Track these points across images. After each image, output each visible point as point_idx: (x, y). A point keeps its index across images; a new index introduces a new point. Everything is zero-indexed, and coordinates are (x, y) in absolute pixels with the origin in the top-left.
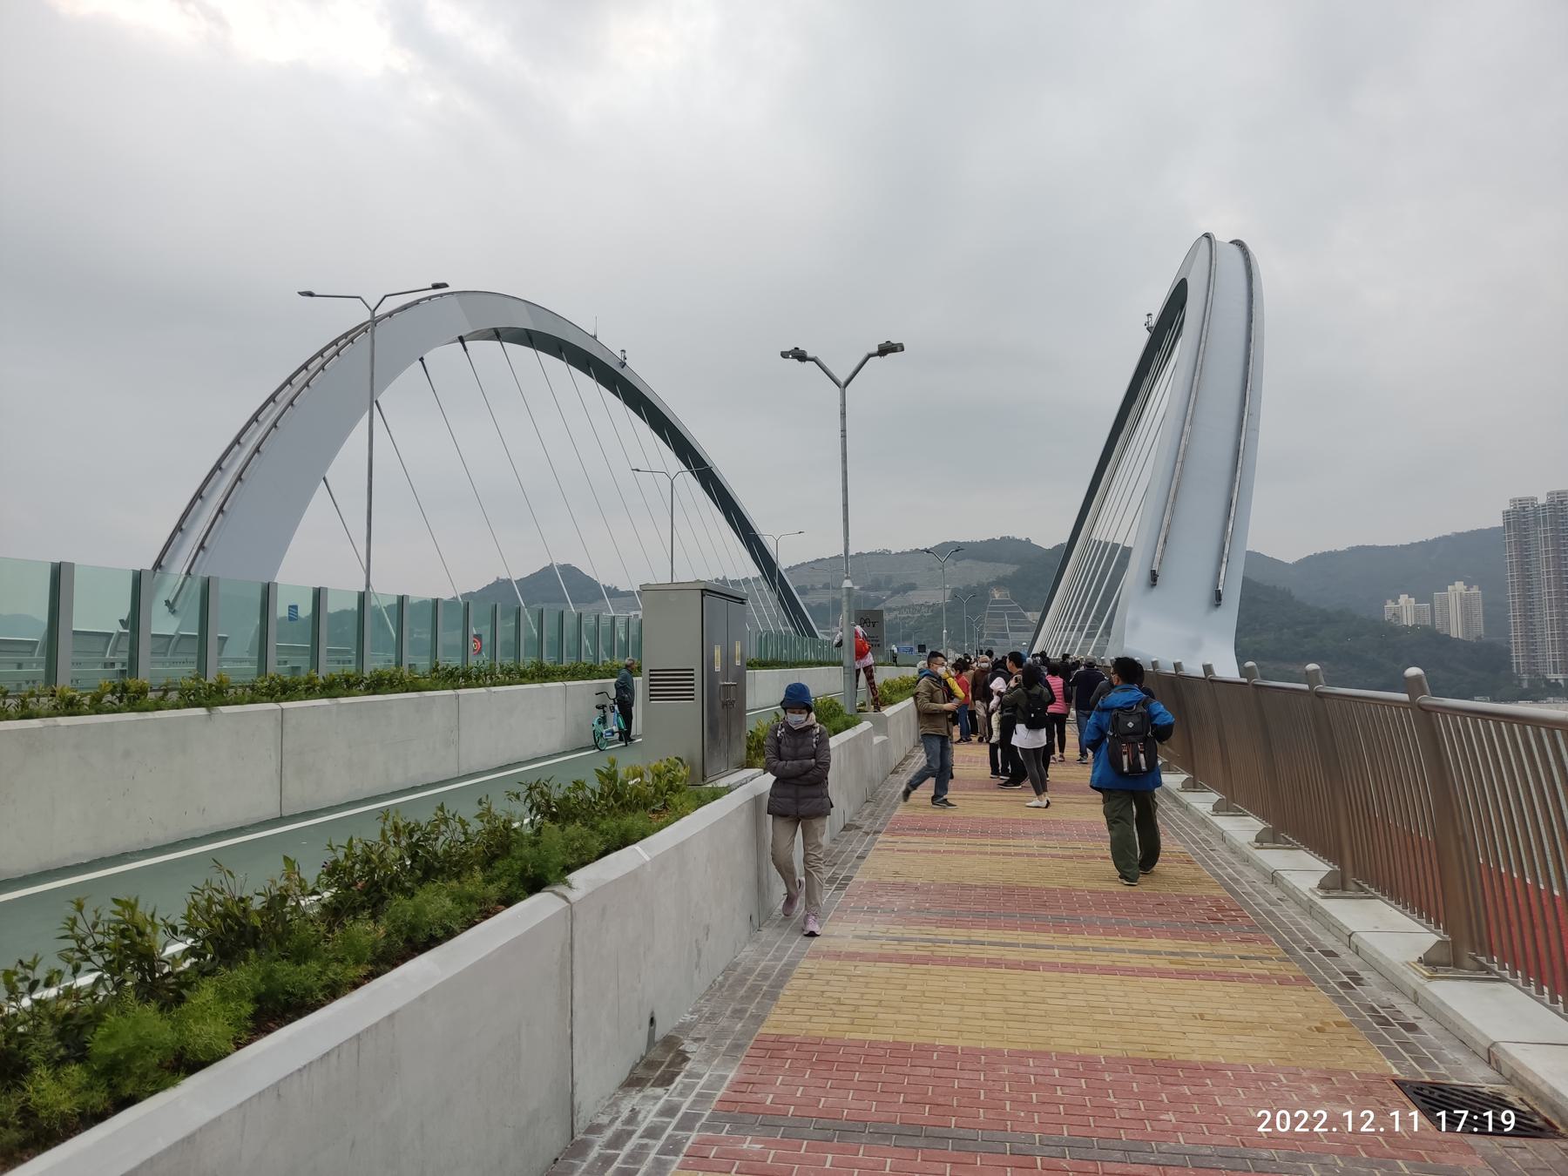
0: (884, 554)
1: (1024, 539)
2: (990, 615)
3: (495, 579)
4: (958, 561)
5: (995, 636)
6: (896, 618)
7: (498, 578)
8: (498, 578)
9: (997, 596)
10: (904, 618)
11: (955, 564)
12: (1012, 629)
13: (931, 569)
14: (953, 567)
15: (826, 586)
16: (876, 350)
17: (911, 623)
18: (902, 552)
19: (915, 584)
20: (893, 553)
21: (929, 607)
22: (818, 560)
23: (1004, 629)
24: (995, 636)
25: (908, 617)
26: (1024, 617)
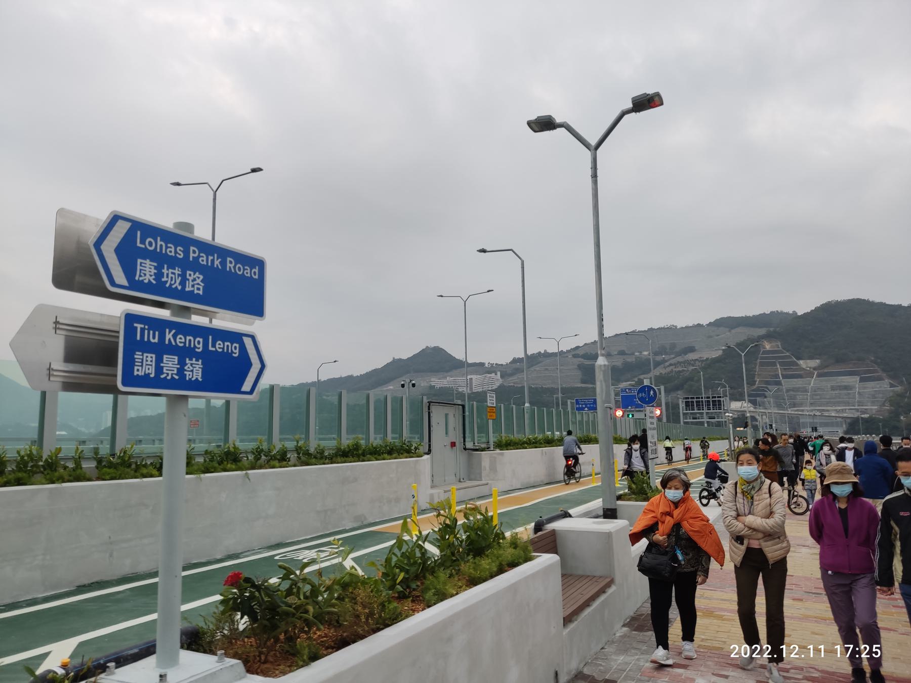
0: (671, 329)
1: (791, 312)
2: (762, 364)
3: (392, 359)
4: (732, 329)
5: (767, 383)
6: (672, 371)
7: (394, 358)
8: (394, 358)
9: (768, 346)
10: (680, 372)
11: (730, 331)
12: (784, 377)
13: (710, 337)
14: (728, 333)
15: (622, 353)
16: (630, 105)
17: (685, 375)
18: (686, 327)
19: (694, 347)
20: (678, 328)
21: (703, 361)
22: (617, 335)
23: (777, 376)
24: (767, 383)
25: (683, 370)
26: (797, 365)
